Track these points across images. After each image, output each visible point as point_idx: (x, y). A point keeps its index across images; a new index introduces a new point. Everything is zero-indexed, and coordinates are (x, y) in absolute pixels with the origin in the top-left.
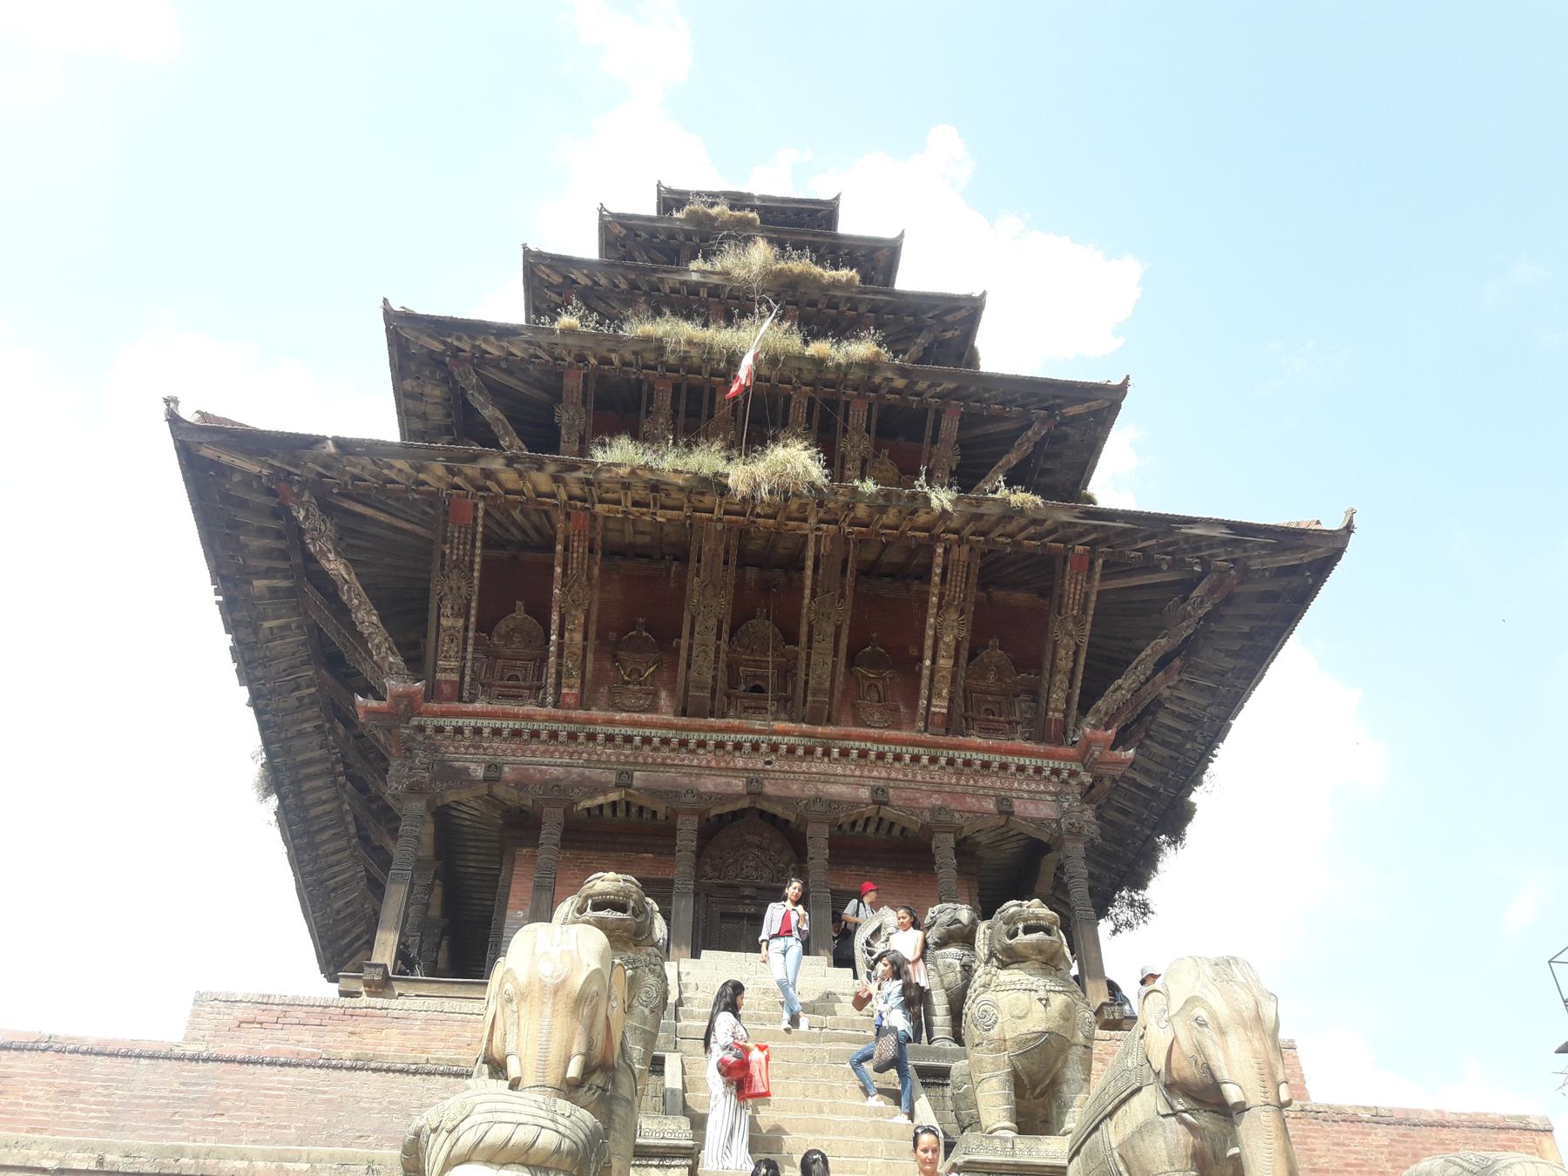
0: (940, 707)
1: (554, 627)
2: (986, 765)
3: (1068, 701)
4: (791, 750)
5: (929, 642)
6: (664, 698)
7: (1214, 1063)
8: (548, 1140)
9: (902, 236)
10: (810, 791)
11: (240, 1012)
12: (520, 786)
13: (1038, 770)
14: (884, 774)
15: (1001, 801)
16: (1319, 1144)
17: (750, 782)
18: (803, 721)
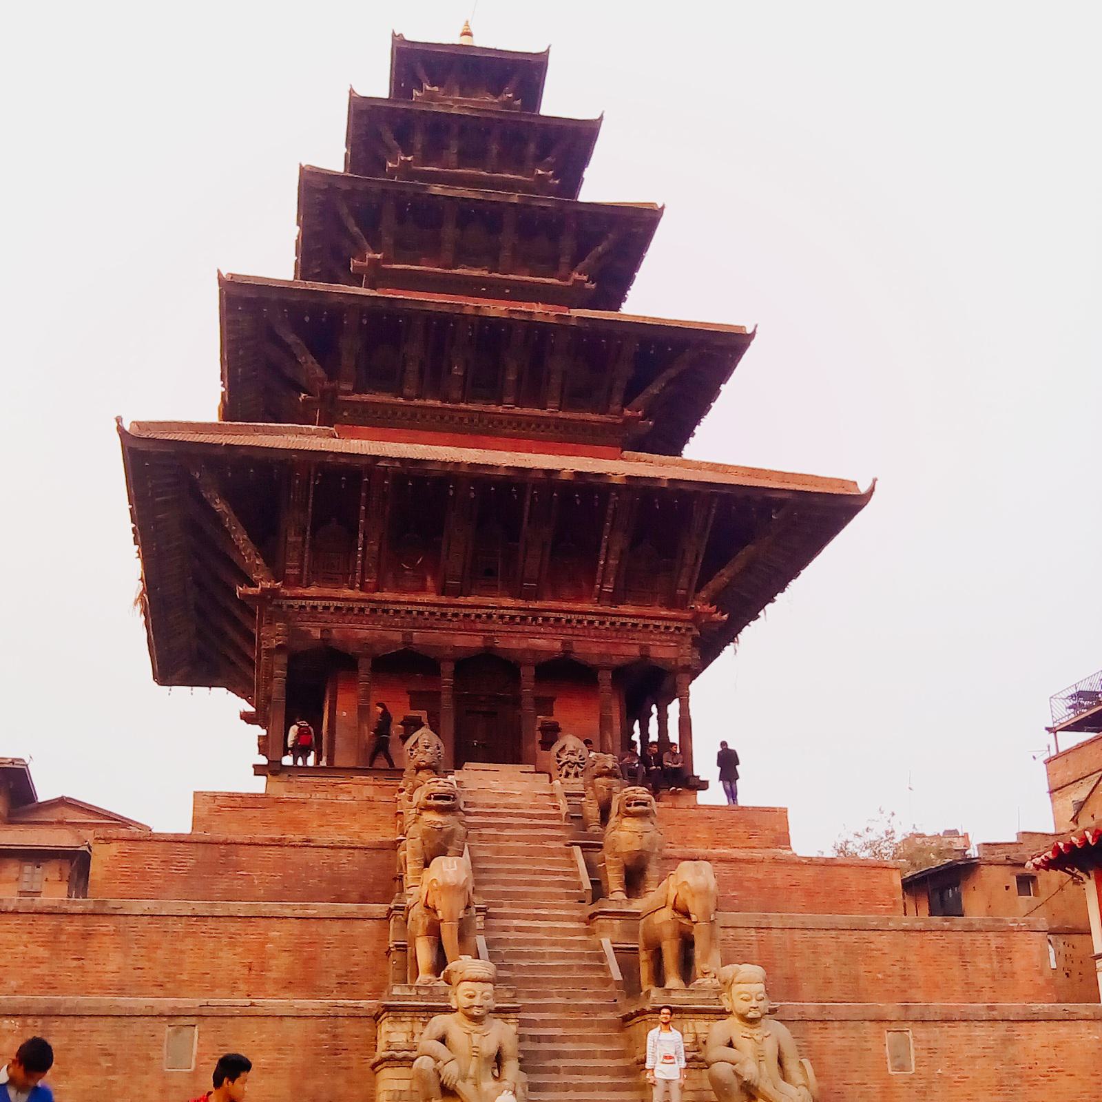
0: (608, 588)
1: (360, 543)
2: (634, 625)
3: (690, 581)
4: (513, 618)
5: (603, 551)
6: (429, 582)
7: (689, 906)
8: (487, 976)
9: (601, 118)
10: (524, 645)
11: (218, 802)
13: (667, 628)
14: (570, 632)
15: (642, 647)
17: (485, 638)
18: (520, 598)
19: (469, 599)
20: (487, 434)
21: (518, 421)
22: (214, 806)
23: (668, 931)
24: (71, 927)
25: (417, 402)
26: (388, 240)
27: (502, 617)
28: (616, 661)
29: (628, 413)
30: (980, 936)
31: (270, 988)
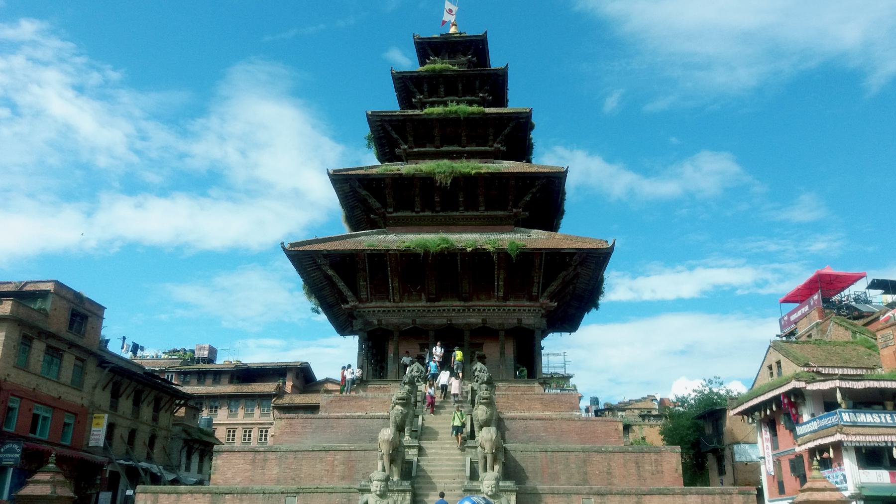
0: (501, 294)
10: (465, 322)
12: (387, 325)
15: (518, 319)
16: (564, 426)
19: (440, 303)
20: (453, 224)
21: (466, 218)
22: (329, 400)
23: (480, 456)
24: (261, 456)
25: (421, 214)
26: (411, 139)
27: (454, 310)
28: (506, 327)
29: (515, 210)
30: (646, 455)
31: (336, 479)
